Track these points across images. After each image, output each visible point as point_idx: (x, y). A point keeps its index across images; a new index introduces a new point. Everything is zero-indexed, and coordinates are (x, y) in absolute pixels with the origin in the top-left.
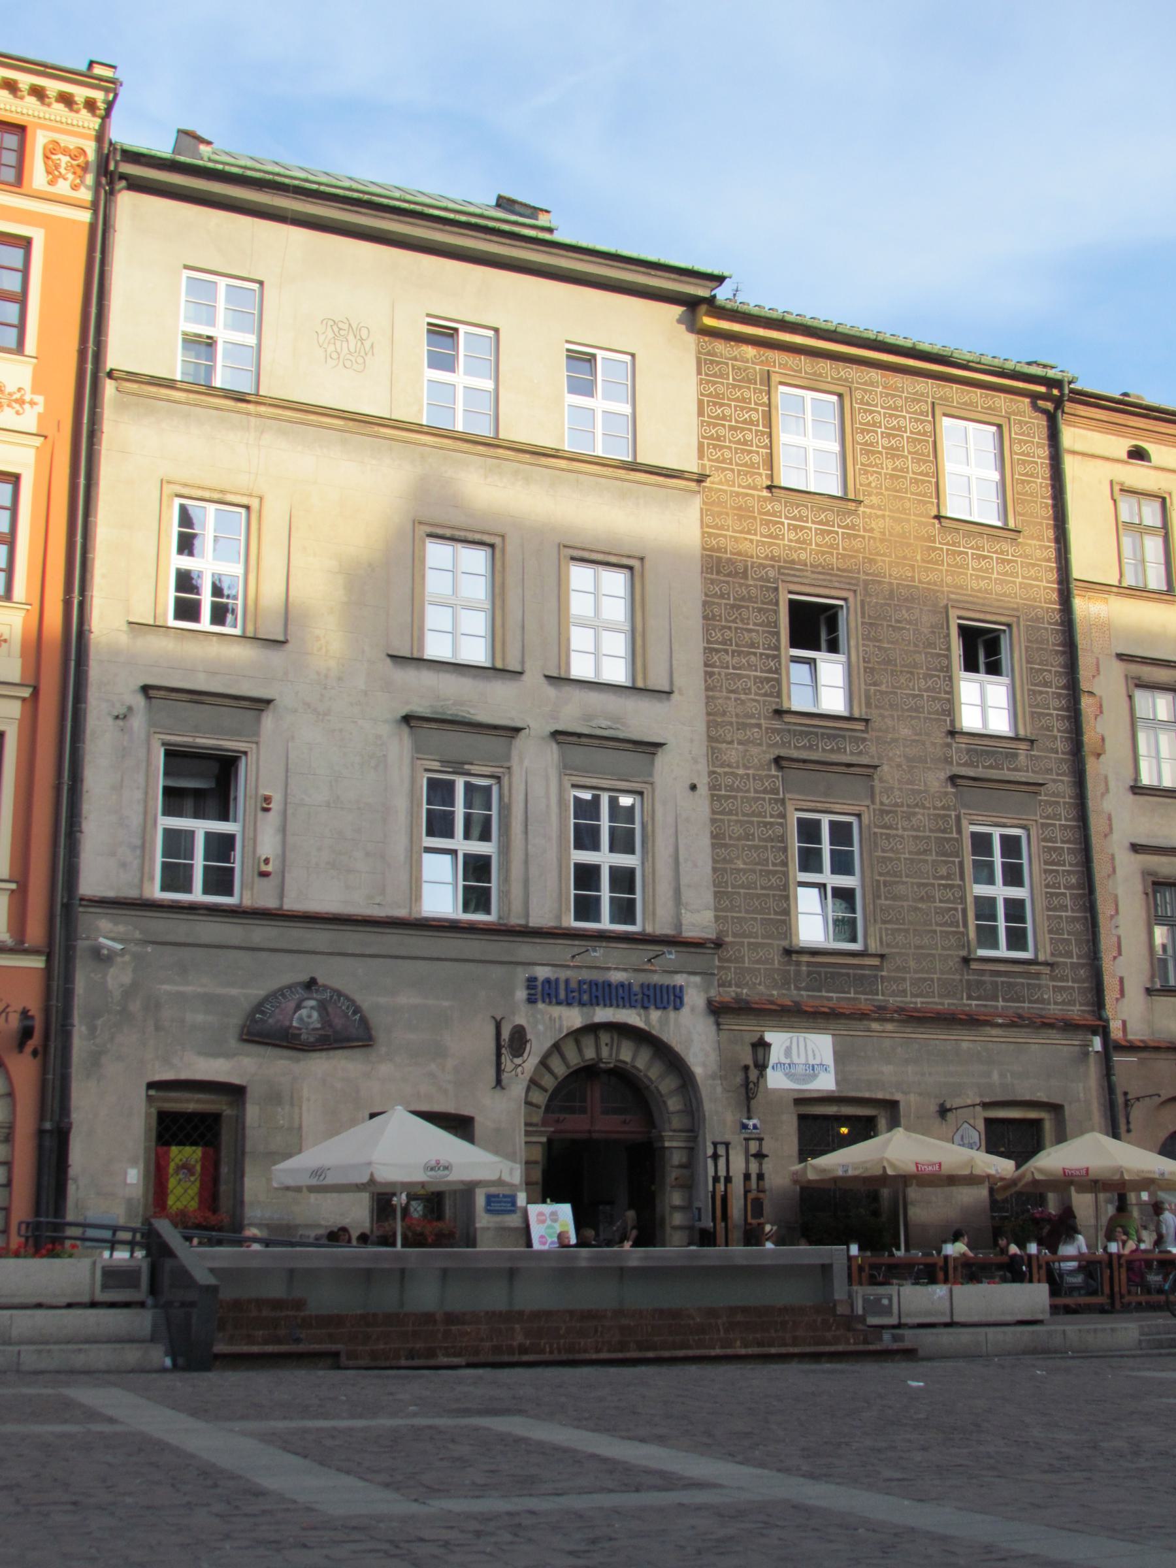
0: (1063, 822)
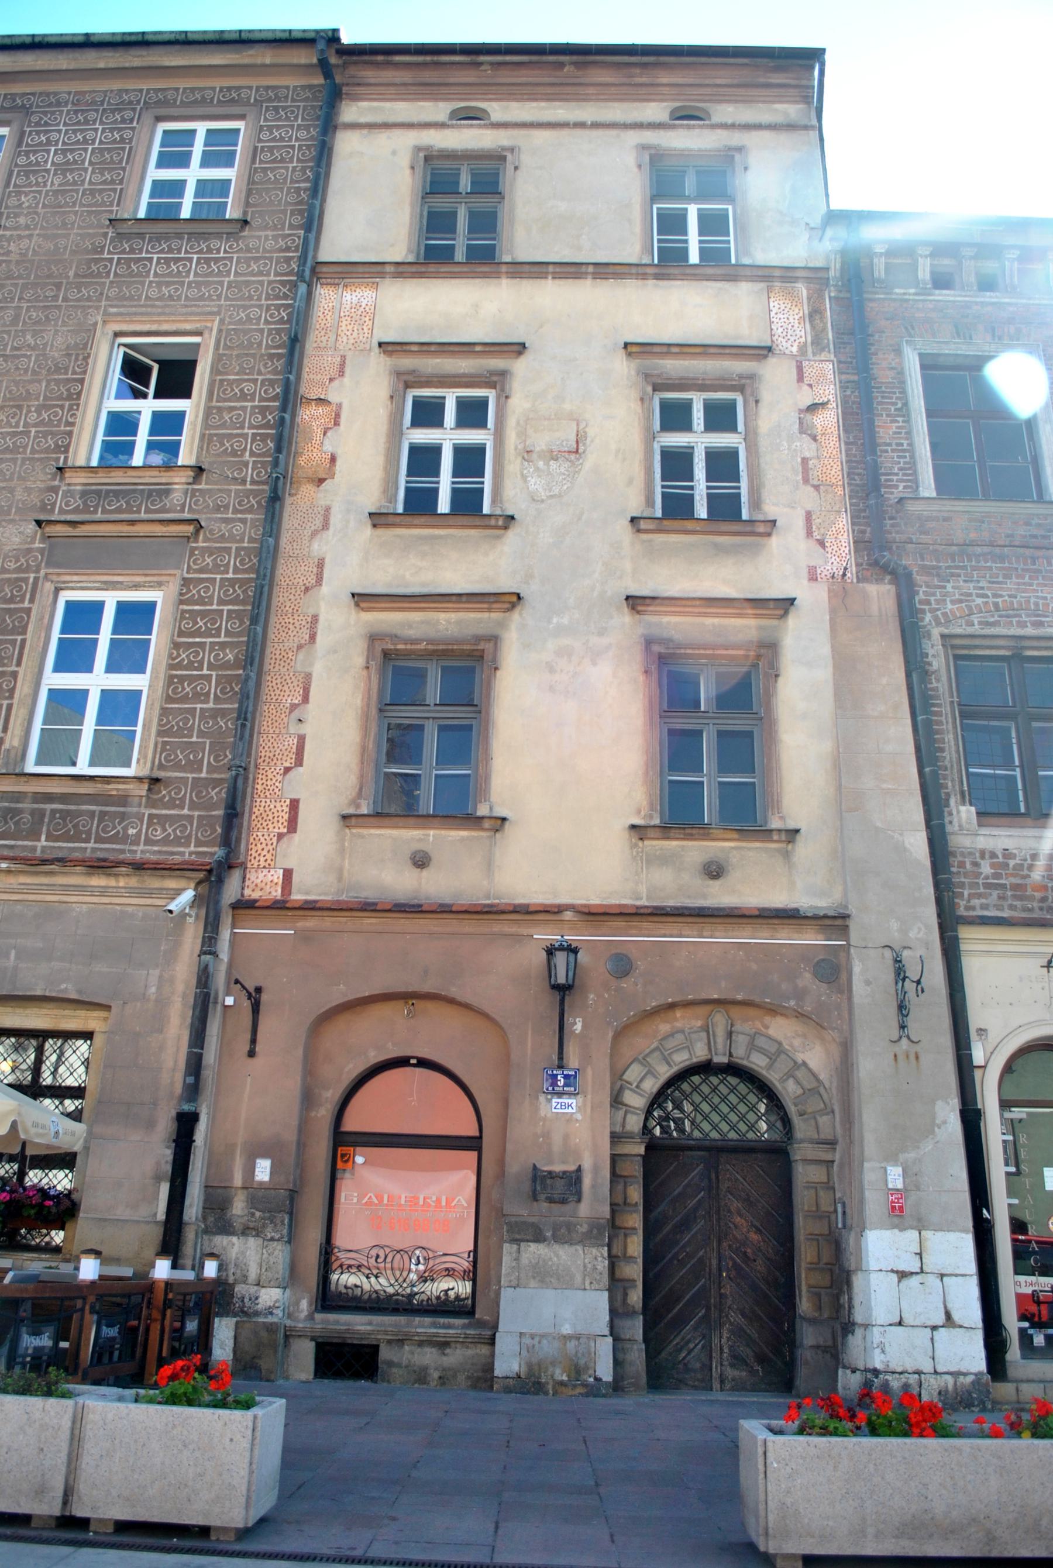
0: (230, 575)
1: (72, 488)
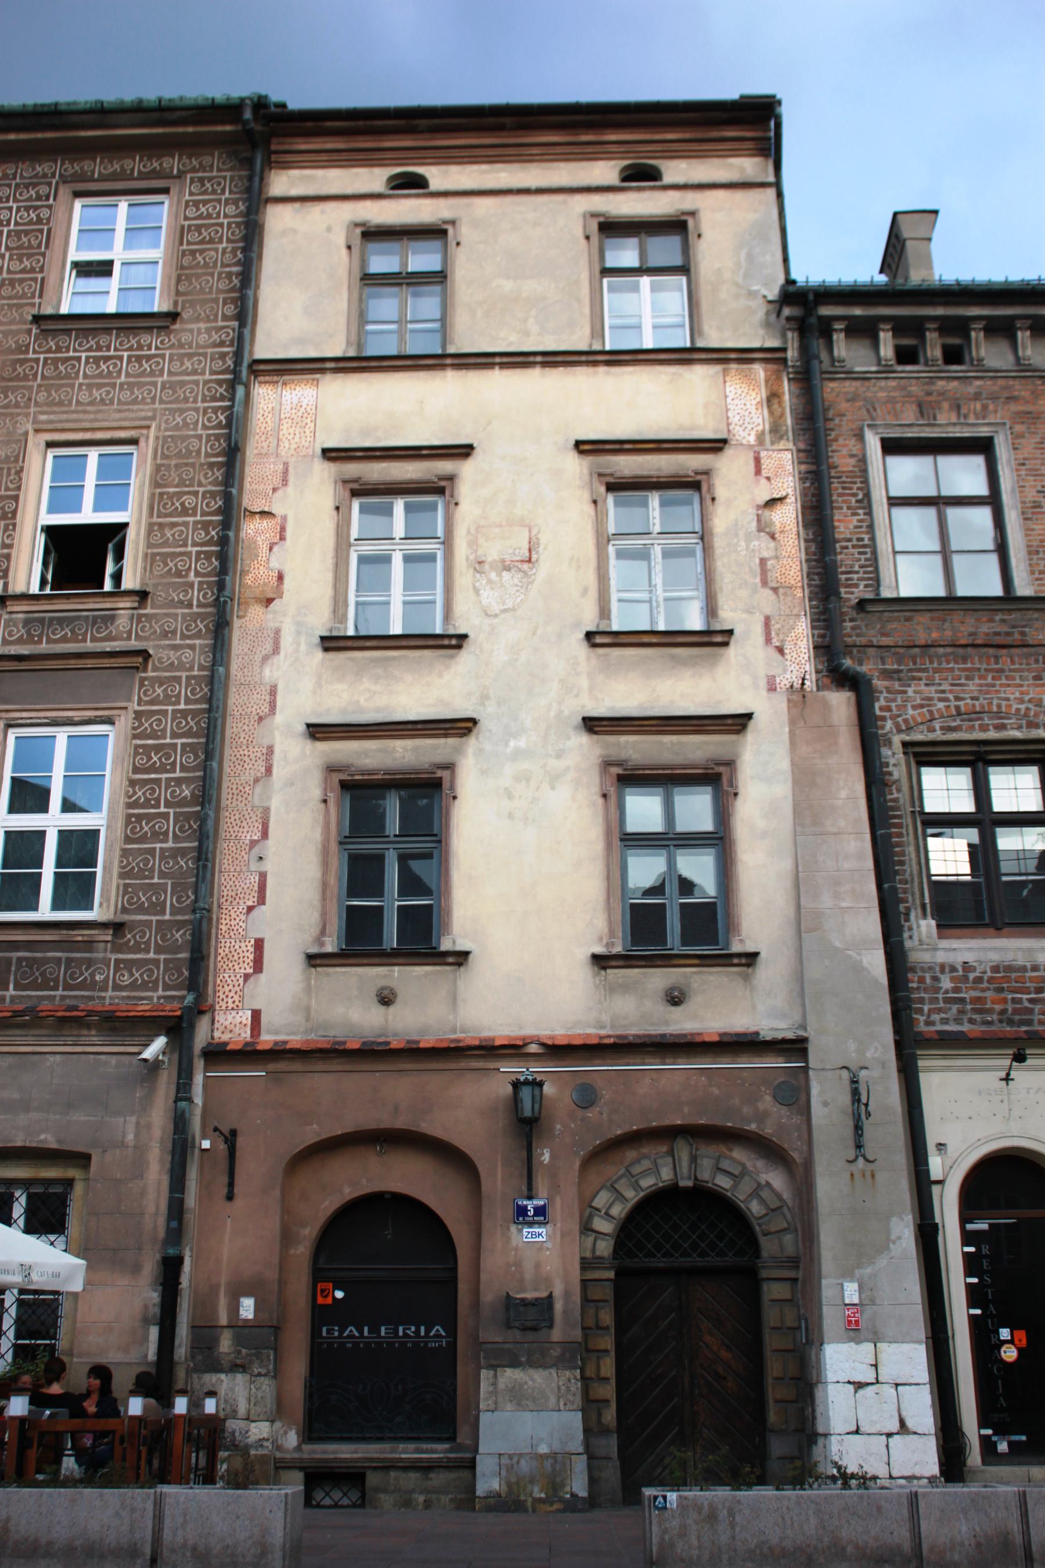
0: (182, 706)
1: (14, 616)
